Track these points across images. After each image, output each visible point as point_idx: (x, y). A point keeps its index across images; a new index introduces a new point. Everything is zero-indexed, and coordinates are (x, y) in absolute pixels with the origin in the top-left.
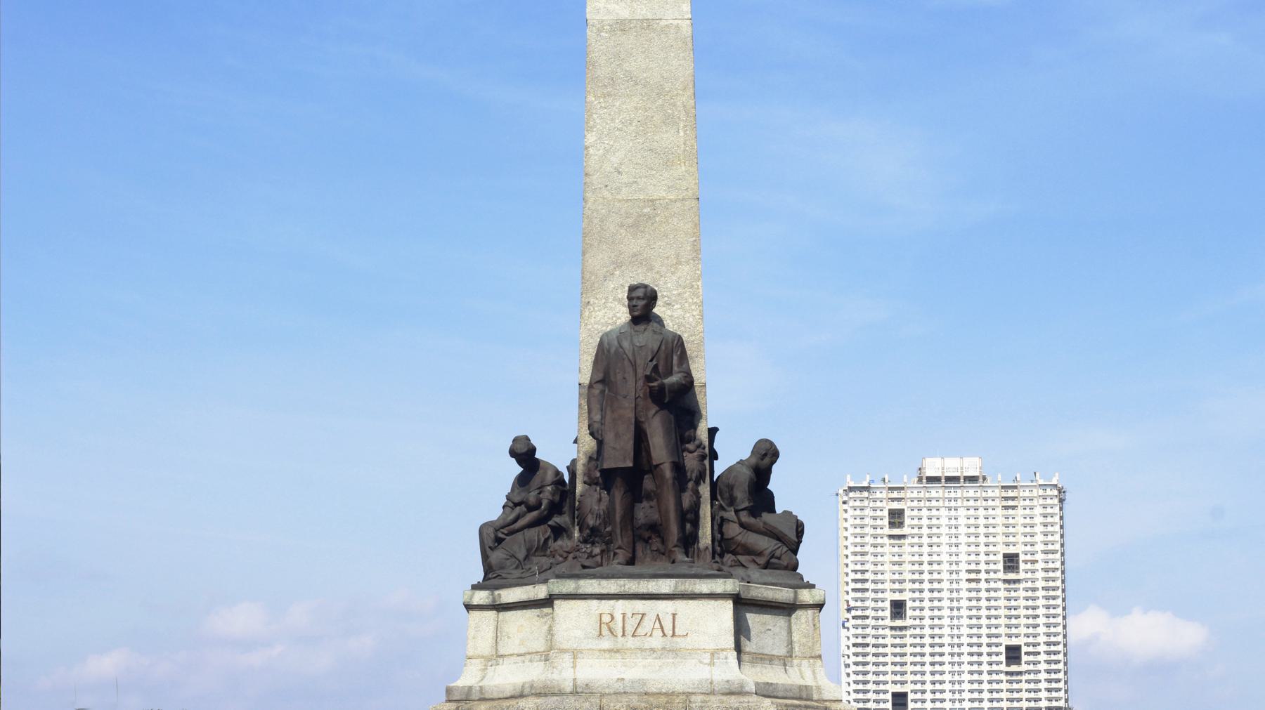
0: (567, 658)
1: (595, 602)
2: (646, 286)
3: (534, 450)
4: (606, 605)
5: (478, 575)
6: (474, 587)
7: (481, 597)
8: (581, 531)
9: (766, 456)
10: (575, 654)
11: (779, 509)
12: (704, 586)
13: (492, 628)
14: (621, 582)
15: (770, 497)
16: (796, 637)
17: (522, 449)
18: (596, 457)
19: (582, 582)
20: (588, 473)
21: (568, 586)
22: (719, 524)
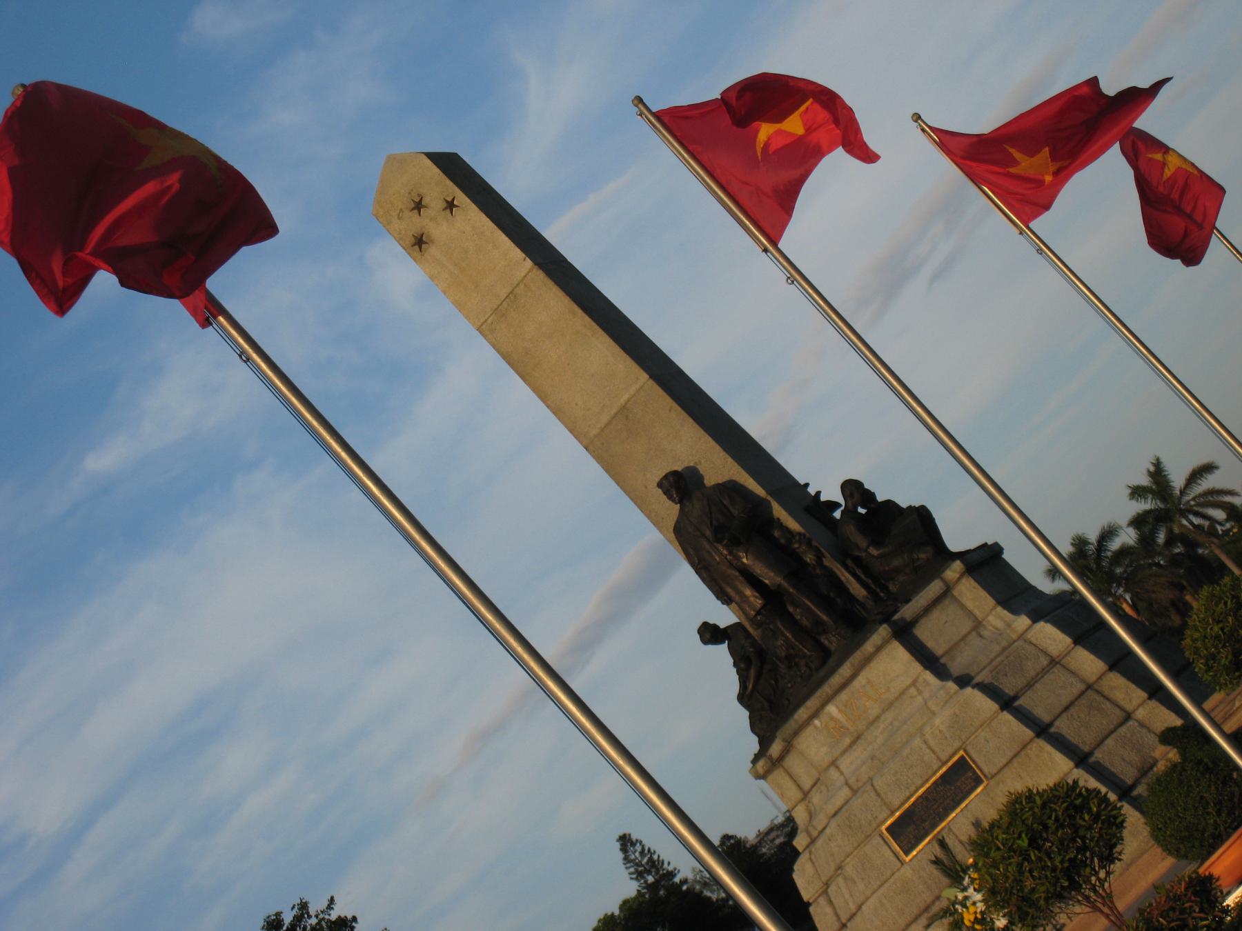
0: (833, 771)
1: (817, 722)
2: (666, 477)
3: (715, 627)
5: (753, 744)
6: (755, 760)
7: (761, 764)
12: (868, 647)
13: (787, 778)
14: (818, 693)
15: (889, 504)
16: (970, 605)
17: (708, 636)
19: (796, 716)
20: (752, 621)
21: (791, 725)
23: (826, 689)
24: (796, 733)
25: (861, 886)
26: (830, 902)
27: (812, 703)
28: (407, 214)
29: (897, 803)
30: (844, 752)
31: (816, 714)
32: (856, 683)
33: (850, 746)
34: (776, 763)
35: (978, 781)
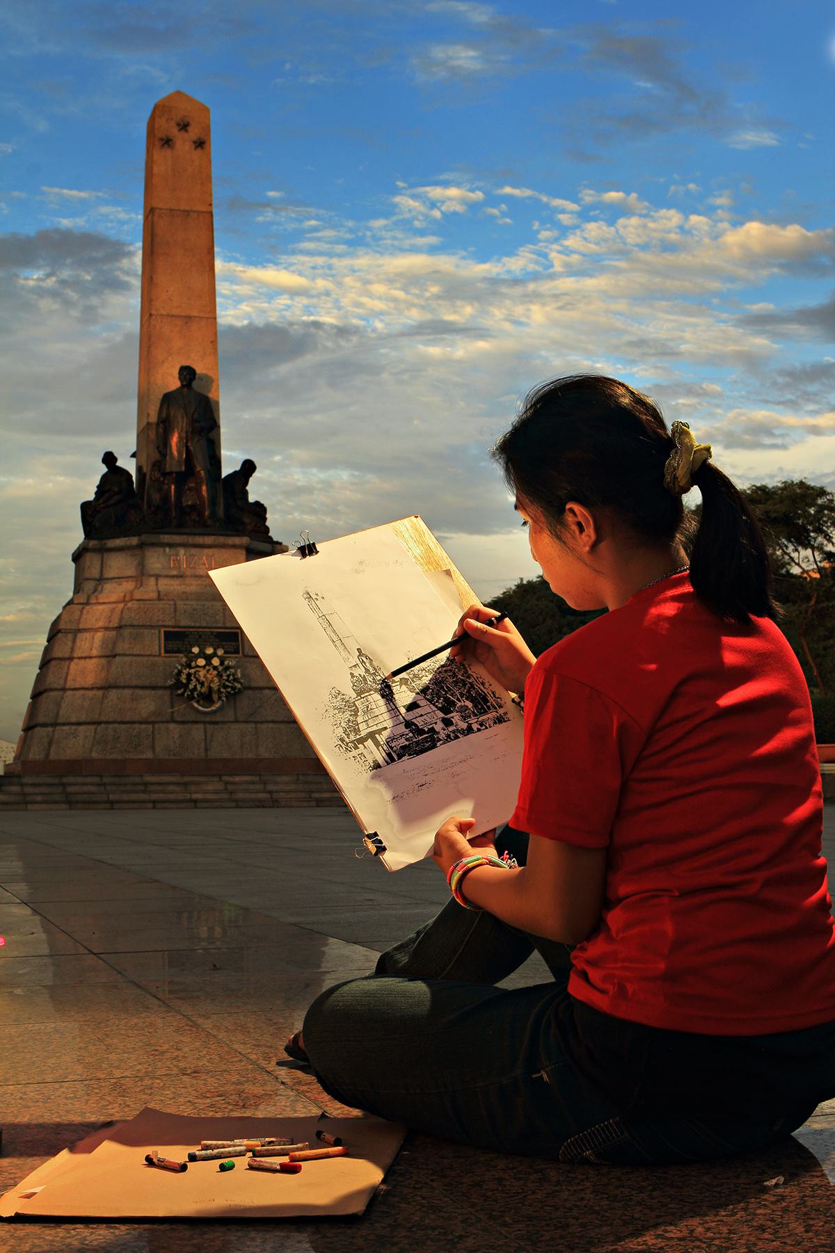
0: (153, 580)
3: (116, 460)
4: (173, 551)
7: (92, 543)
8: (149, 507)
9: (248, 468)
10: (157, 577)
11: (252, 499)
14: (184, 537)
18: (158, 465)
22: (227, 509)
23: (191, 539)
24: (153, 545)
25: (127, 646)
26: (74, 641)
27: (177, 539)
28: (173, 123)
29: (182, 624)
30: (167, 576)
31: (171, 545)
32: (206, 551)
33: (173, 577)
34: (103, 551)
35: (237, 652)
